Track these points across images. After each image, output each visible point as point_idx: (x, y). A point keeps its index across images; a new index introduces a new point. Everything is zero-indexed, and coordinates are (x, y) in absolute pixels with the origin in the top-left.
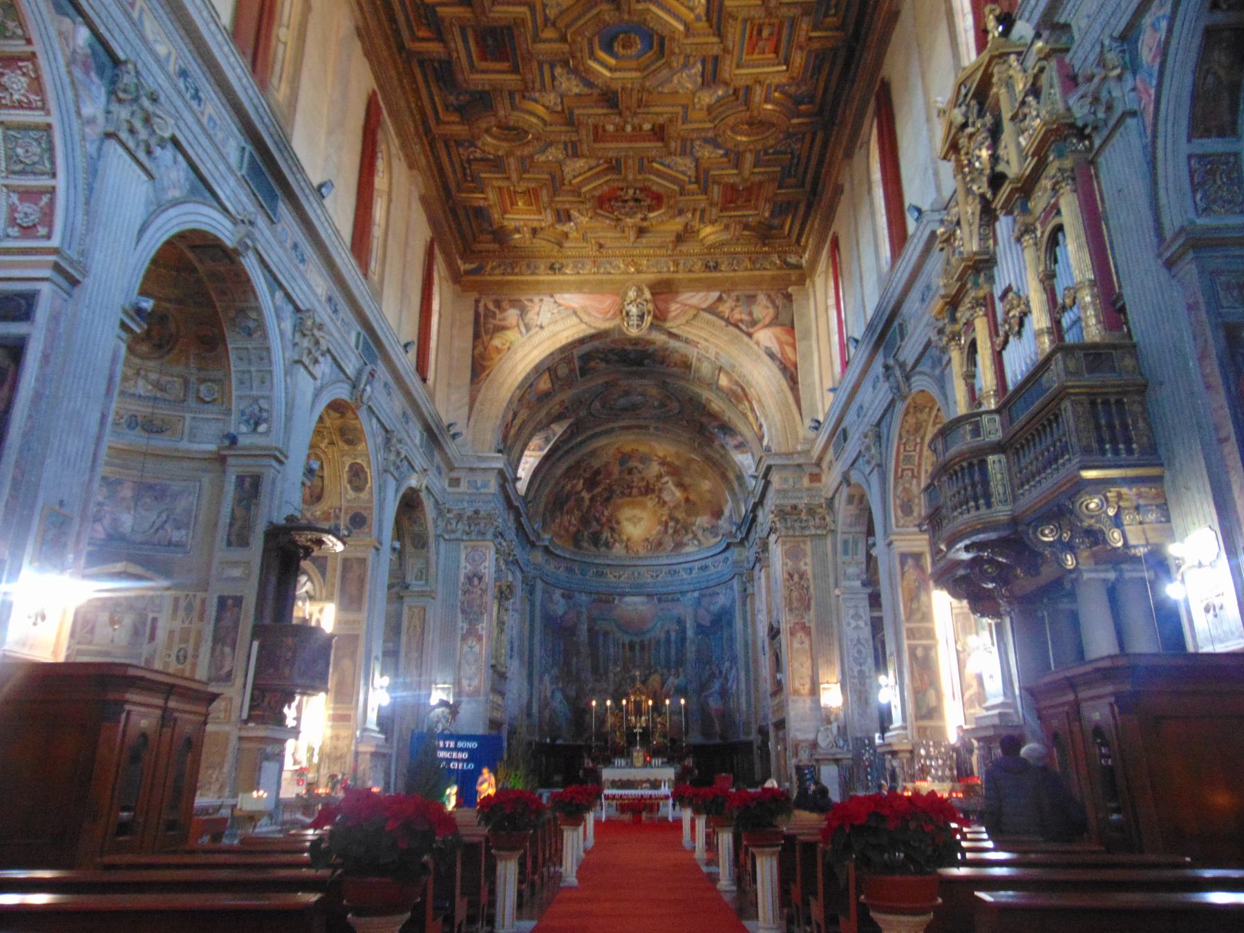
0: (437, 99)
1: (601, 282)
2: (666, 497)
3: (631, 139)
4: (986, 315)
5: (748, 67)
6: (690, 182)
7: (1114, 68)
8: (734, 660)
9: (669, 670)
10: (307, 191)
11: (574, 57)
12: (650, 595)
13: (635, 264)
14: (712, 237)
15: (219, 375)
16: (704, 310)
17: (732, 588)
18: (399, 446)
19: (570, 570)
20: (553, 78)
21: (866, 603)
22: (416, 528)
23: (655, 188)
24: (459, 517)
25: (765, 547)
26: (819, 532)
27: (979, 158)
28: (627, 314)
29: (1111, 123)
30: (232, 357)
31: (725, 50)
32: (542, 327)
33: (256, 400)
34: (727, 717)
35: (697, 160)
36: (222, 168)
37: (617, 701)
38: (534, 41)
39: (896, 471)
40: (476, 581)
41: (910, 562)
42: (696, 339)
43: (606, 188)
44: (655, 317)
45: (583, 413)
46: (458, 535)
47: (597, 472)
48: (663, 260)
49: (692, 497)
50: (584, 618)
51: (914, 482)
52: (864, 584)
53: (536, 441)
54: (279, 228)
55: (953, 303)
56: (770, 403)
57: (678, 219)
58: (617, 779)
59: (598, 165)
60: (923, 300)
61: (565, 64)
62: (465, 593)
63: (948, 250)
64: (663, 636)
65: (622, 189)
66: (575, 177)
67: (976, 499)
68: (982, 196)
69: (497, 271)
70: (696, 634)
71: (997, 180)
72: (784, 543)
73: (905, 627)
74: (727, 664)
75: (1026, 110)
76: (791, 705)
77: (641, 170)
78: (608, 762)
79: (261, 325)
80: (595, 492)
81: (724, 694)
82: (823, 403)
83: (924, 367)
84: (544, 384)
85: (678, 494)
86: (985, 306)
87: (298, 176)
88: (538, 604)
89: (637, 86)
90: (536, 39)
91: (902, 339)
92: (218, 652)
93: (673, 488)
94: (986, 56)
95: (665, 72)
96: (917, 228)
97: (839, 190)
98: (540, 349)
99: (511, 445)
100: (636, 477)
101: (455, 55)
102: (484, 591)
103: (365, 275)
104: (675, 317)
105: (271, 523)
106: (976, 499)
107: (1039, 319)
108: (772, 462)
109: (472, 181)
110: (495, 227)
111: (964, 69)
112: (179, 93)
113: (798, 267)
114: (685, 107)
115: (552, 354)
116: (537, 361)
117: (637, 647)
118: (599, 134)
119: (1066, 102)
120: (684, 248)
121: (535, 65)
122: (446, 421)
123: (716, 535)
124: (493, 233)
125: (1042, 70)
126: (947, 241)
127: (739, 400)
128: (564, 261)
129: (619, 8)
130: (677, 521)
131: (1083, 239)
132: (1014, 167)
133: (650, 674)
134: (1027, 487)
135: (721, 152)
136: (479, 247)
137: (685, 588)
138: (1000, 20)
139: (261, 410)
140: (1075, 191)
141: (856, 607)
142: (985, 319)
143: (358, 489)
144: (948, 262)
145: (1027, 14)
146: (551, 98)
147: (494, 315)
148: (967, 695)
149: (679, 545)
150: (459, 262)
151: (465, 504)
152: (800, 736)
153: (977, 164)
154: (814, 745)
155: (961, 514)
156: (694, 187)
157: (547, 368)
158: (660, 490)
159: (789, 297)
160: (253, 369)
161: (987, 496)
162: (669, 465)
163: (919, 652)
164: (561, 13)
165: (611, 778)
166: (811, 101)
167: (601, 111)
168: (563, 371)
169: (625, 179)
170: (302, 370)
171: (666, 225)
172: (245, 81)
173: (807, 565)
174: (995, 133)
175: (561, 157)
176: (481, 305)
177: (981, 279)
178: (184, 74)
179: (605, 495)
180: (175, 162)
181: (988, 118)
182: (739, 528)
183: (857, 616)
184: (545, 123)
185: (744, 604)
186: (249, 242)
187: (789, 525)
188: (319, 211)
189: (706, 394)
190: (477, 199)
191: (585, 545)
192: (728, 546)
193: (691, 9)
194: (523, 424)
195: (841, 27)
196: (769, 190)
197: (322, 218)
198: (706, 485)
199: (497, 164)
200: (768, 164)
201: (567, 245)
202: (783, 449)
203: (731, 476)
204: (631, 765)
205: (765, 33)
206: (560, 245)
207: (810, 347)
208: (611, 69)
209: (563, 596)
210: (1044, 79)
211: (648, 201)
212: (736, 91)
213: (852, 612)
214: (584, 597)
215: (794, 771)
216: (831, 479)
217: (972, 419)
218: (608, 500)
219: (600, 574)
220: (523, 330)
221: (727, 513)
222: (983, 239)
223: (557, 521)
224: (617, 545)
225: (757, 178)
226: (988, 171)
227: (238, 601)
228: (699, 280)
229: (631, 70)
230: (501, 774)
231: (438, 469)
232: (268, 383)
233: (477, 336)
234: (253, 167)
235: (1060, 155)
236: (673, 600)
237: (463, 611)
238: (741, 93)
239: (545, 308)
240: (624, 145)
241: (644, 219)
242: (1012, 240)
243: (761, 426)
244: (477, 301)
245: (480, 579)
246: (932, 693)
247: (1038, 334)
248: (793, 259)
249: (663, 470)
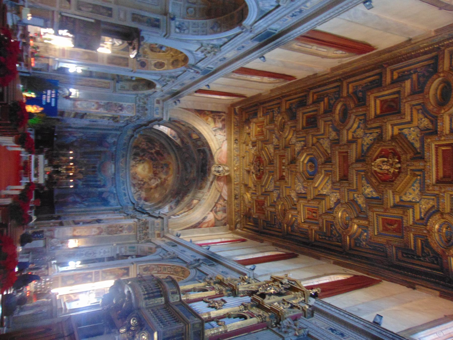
1: (231, 157)
2: (153, 181)
3: (280, 168)
4: (216, 294)
6: (265, 189)
7: (299, 333)
8: (88, 206)
9: (84, 182)
11: (307, 149)
12: (115, 174)
13: (237, 170)
14: (246, 197)
15: (197, 16)
17: (117, 205)
18: (171, 81)
19: (125, 144)
20: (300, 141)
21: (110, 256)
22: (140, 86)
23: (263, 176)
24: (145, 103)
25: (132, 217)
26: (138, 237)
27: (271, 289)
28: (219, 167)
29: (280, 333)
30: (204, 21)
31: (309, 201)
32: (215, 135)
33: (188, 28)
34: (65, 204)
35: (272, 192)
36: (270, 22)
37: (72, 161)
38: (312, 135)
39: (160, 265)
40: (120, 108)
41: (126, 271)
42: (210, 191)
43: (263, 159)
44: (218, 177)
45: (184, 150)
46: (138, 103)
47: (162, 155)
48: (239, 180)
49: (152, 190)
50: (105, 149)
51: (156, 272)
52: (117, 255)
53: (174, 133)
54: (250, 42)
55: (221, 283)
56: (187, 219)
57: (252, 185)
58: (39, 161)
60: (222, 272)
61: (305, 145)
62: (115, 104)
63: (239, 280)
64: (98, 179)
67: (147, 294)
70: (99, 192)
71: (263, 296)
72: (134, 224)
73: (100, 270)
74: (86, 204)
75: (286, 304)
76: (70, 228)
77: (270, 172)
78: (46, 157)
79: (215, 32)
80: (155, 155)
81: (75, 203)
82: (186, 238)
83: (198, 274)
84: (195, 136)
85: (154, 185)
87: (267, 50)
88: (110, 132)
89: (297, 170)
90: (313, 136)
91: (209, 265)
92: (90, 6)
93: (156, 183)
94: (304, 289)
95: (302, 180)
96: (247, 269)
97: (262, 241)
98: (207, 135)
99: (172, 123)
100: (160, 170)
101: (308, 107)
102: (116, 111)
103: (233, 72)
104: (218, 184)
105: (141, 31)
106: (147, 294)
107: (214, 313)
108: (165, 219)
109: (266, 112)
110: (251, 120)
112: (294, 9)
113: (236, 228)
114: (290, 187)
115: (205, 139)
116: (203, 134)
117: (94, 169)
118: (282, 157)
119: (288, 317)
120: (243, 187)
121: (305, 135)
122: (181, 99)
123: (138, 199)
126: (243, 279)
127: (188, 207)
128: (238, 144)
129: (322, 164)
130: (143, 185)
131: (242, 327)
132: (267, 301)
133: (83, 174)
134: (152, 312)
135: (275, 200)
136: (244, 113)
137: (117, 187)
138: (316, 293)
139: (184, 30)
140: (258, 323)
141: (108, 252)
142: (215, 294)
143: (155, 65)
144: (236, 280)
145: (317, 302)
146: (294, 140)
147: (220, 118)
148: (72, 296)
149: (134, 185)
151: (149, 106)
152: (56, 232)
153: (269, 289)
154: (52, 237)
155: (142, 289)
156: (264, 190)
157: (201, 138)
158: (155, 179)
159: (225, 225)
160: (199, 28)
161: (149, 298)
162: (165, 181)
163: (89, 276)
164: (321, 144)
165: (39, 158)
166: (292, 231)
167: (289, 157)
168: (199, 143)
169: (266, 166)
170: (199, 47)
171: (251, 181)
172: (299, 33)
173: (125, 233)
174: (279, 294)
175: (274, 143)
176: (223, 114)
177: (229, 292)
178: (301, 11)
179: (153, 158)
180: (272, 6)
181: (284, 292)
182: (140, 208)
183: (105, 252)
185: (111, 210)
186: (244, 30)
187: (141, 226)
188: (255, 56)
189: (190, 195)
190: (260, 114)
191: (135, 150)
192: (134, 204)
193: (322, 189)
194: (180, 128)
195: (315, 240)
196: (263, 217)
197: (253, 57)
198: (157, 195)
199: (272, 121)
200: (271, 216)
201: (244, 145)
202: (170, 224)
203: (160, 205)
204: (45, 166)
205: (314, 214)
206: (244, 143)
207: (207, 233)
208: (303, 161)
209: (115, 142)
210: (296, 309)
212: (295, 205)
213: (107, 250)
214: (114, 149)
215: (41, 230)
216: (158, 241)
217: (178, 292)
218: (152, 159)
219: (123, 156)
220: (214, 129)
221: (146, 203)
222: (243, 292)
223: (144, 140)
224: (134, 162)
225: (266, 213)
226: (266, 292)
227: (110, 15)
228: (231, 192)
229: (303, 168)
230: (42, 115)
231: (163, 96)
232: (195, 33)
233: (212, 112)
235: (270, 317)
236: (113, 183)
237: (108, 103)
238: (294, 207)
239: (222, 137)
240: (278, 166)
241: (253, 173)
242: (241, 303)
243: (178, 215)
244: (224, 113)
245: (121, 110)
246: (73, 282)
247: (209, 313)
248: (238, 226)
249: (163, 180)
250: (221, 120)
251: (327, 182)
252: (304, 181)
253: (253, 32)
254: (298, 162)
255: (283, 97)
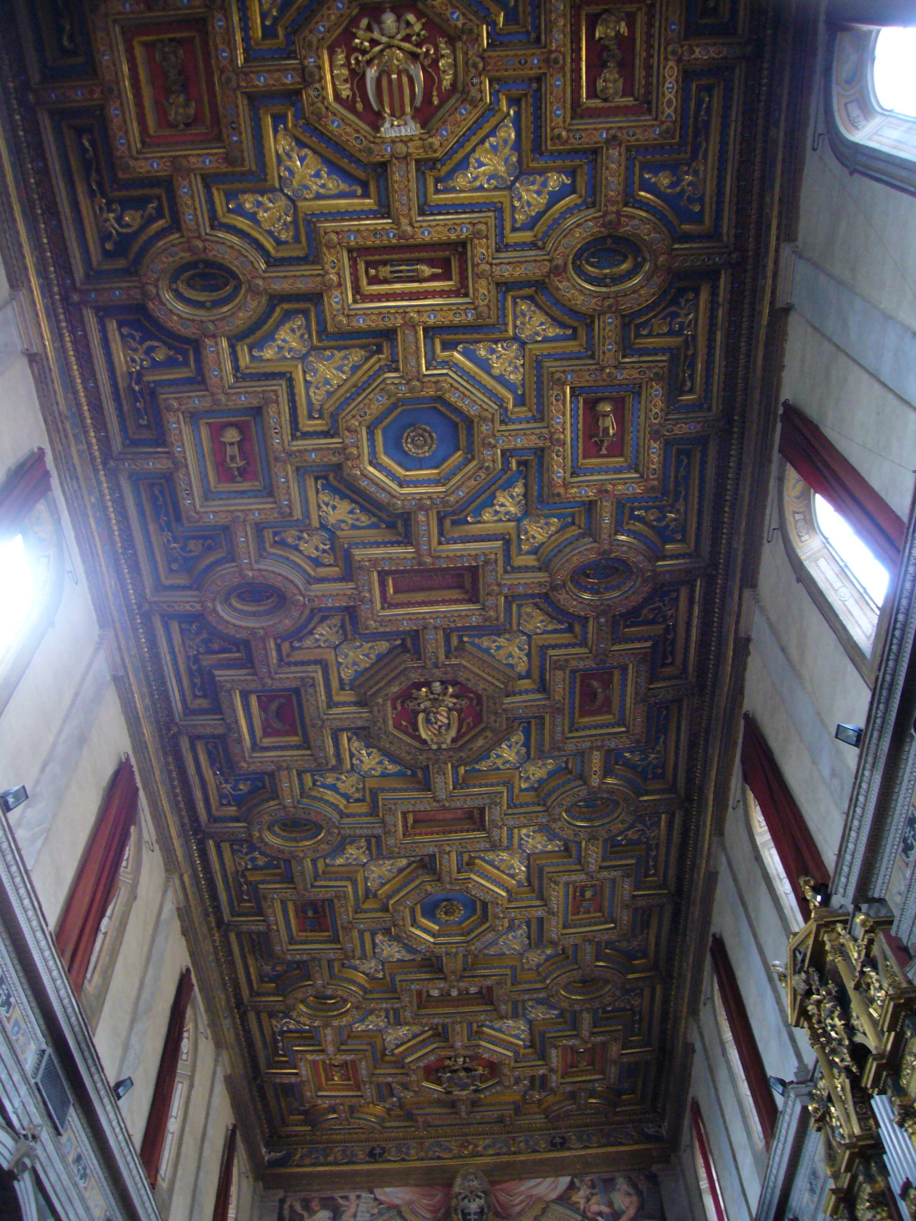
0: (252, 970)
3: (456, 1002)
5: (575, 927)
10: (103, 1093)
16: (554, 1201)
20: (374, 945)
23: (486, 1056)
27: (833, 1027)
31: (551, 913)
36: (16, 1077)
54: (64, 1139)
59: (424, 1032)
60: (812, 1190)
61: (387, 932)
65: (450, 1058)
66: (398, 1046)
68: (847, 1069)
69: (307, 1161)
86: (886, 1205)
94: (812, 925)
96: (786, 1104)
97: (690, 1049)
103: (153, 1186)
111: (795, 934)
114: (514, 968)
119: (905, 976)
121: (355, 934)
124: (305, 1113)
125: (871, 942)
138: (816, 890)
145: (841, 890)
146: (371, 965)
150: (264, 1150)
153: (833, 1034)
159: (653, 1179)
169: (452, 1047)
172: (59, 982)
174: (842, 1000)
176: (286, 1206)
184: (365, 991)
186: (27, 1161)
188: (112, 1115)
193: (512, 876)
197: (115, 1123)
199: (311, 1037)
205: (588, 894)
210: (875, 951)
211: (480, 1070)
225: (599, 1039)
228: (543, 1162)
234: (50, 1074)
239: (363, 1207)
242: (896, 1126)
244: (282, 1201)
248: (650, 1130)
250: (305, 1214)
251: (491, 863)
252: (492, 928)
253: (36, 1133)
254: (437, 950)
255: (239, 1003)
